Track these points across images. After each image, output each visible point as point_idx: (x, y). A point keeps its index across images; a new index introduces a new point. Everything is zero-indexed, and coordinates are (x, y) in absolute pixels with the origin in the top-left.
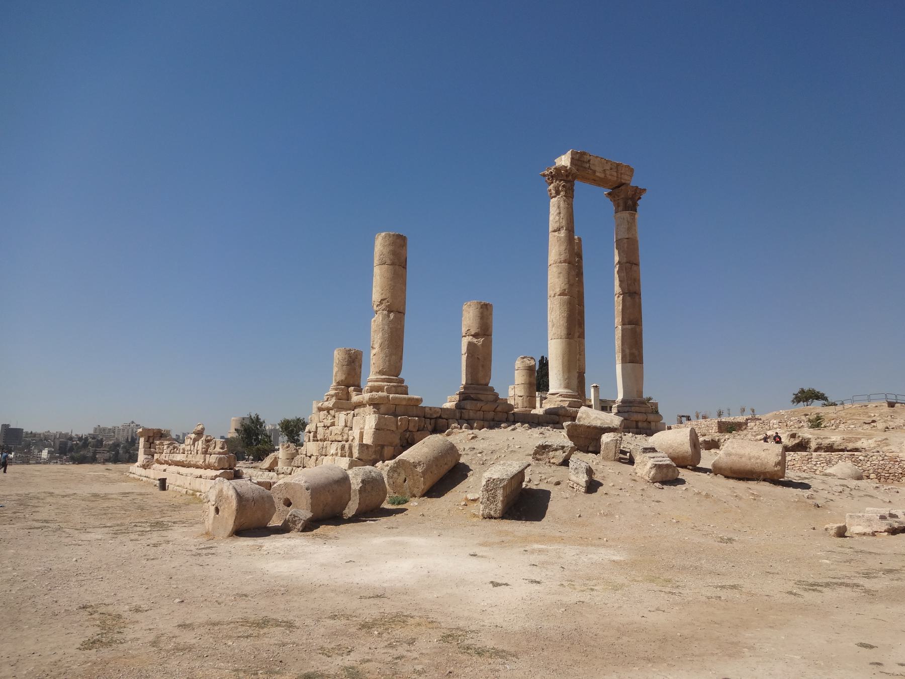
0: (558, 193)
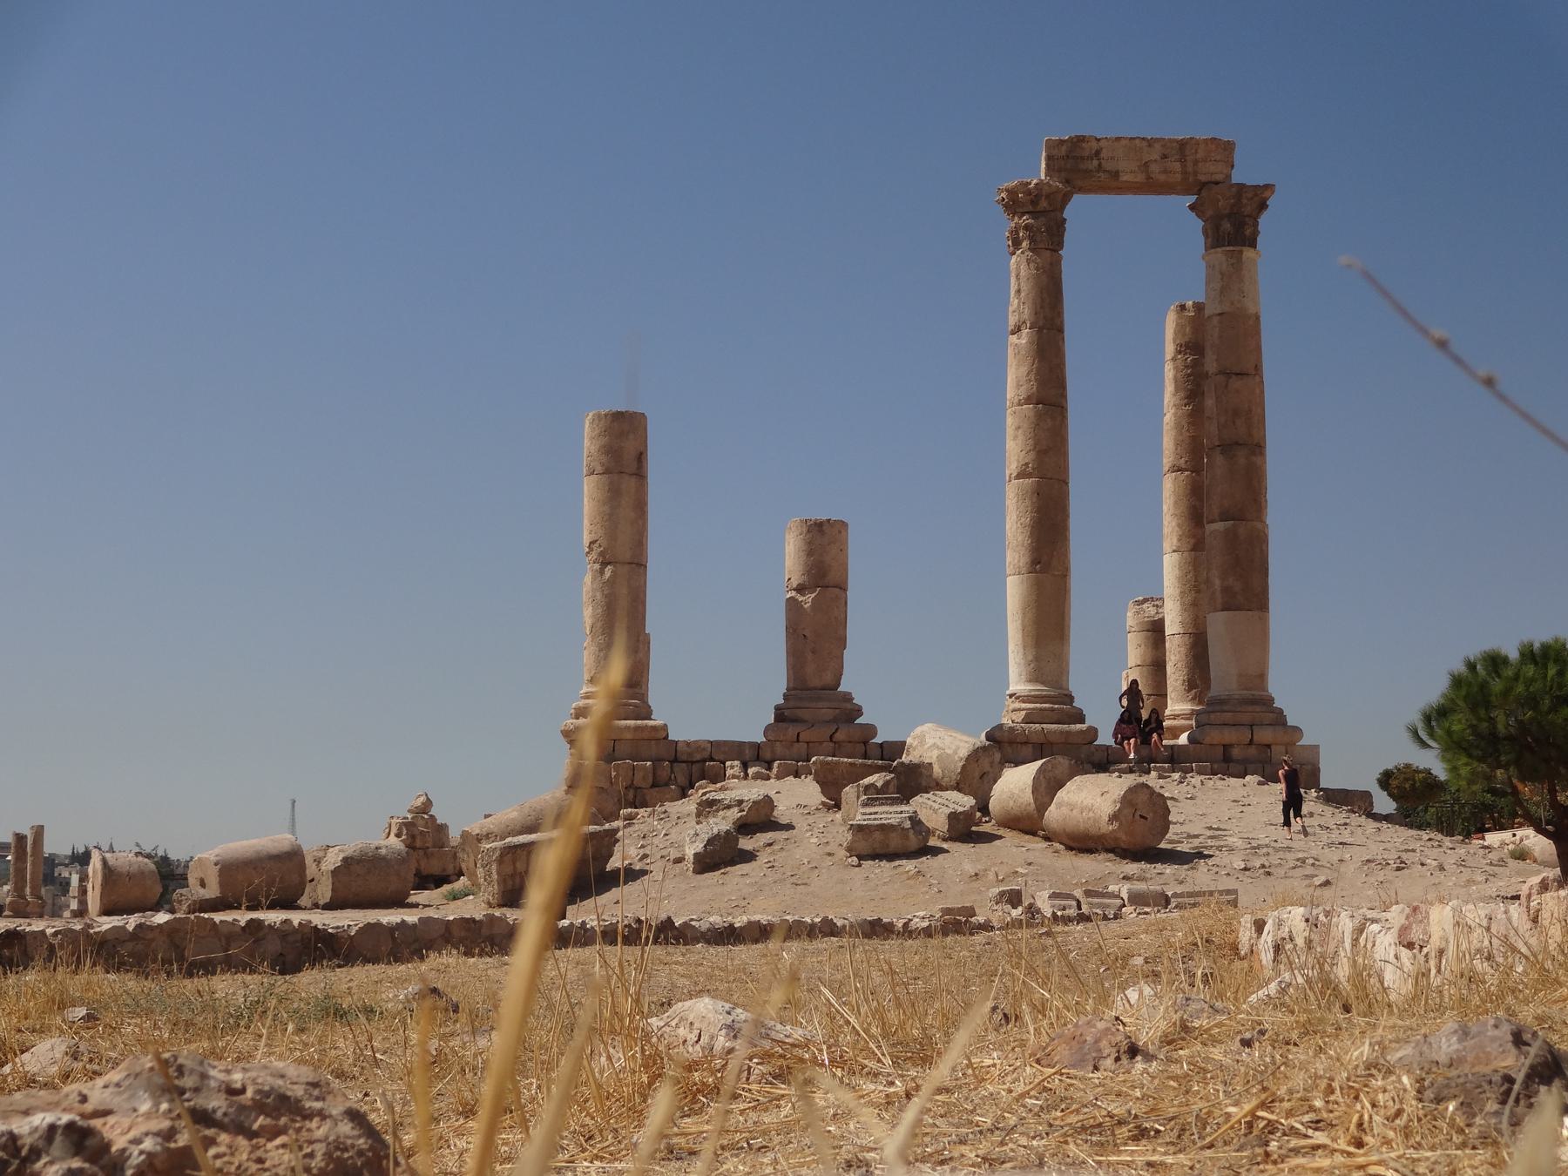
0: (1017, 243)
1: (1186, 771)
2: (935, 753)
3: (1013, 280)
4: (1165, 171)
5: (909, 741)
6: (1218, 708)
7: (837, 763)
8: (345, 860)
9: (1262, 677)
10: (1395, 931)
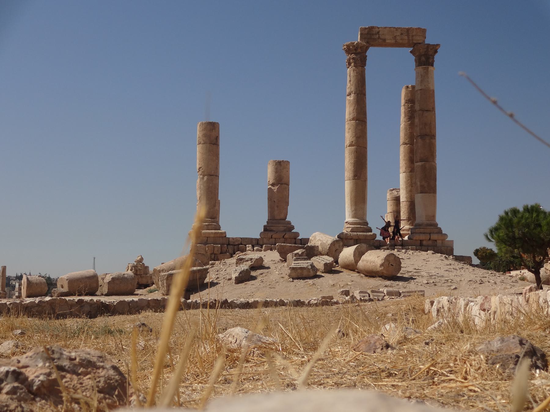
0: (350, 64)
1: (407, 249)
2: (320, 242)
3: (348, 77)
4: (402, 39)
5: (311, 238)
6: (418, 227)
7: (285, 246)
8: (113, 278)
9: (434, 216)
10: (479, 305)
